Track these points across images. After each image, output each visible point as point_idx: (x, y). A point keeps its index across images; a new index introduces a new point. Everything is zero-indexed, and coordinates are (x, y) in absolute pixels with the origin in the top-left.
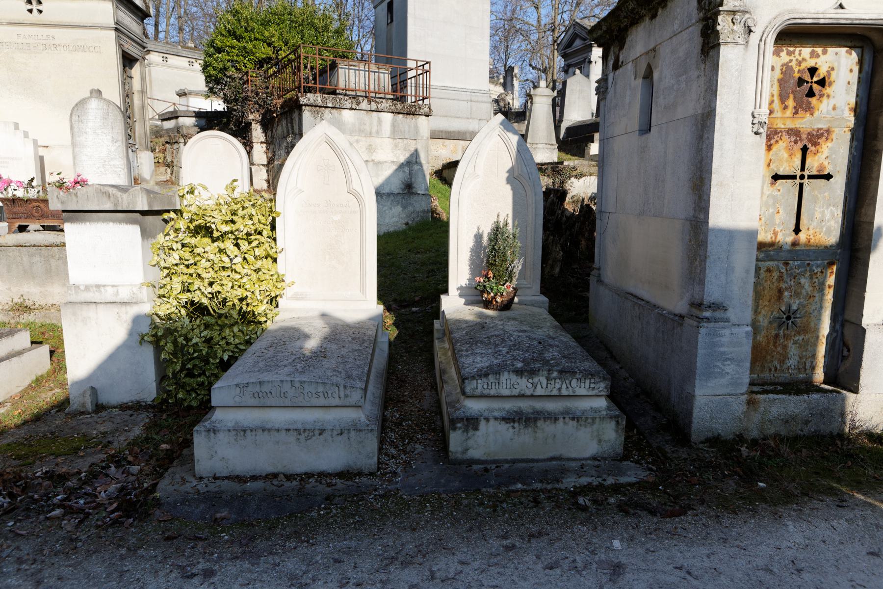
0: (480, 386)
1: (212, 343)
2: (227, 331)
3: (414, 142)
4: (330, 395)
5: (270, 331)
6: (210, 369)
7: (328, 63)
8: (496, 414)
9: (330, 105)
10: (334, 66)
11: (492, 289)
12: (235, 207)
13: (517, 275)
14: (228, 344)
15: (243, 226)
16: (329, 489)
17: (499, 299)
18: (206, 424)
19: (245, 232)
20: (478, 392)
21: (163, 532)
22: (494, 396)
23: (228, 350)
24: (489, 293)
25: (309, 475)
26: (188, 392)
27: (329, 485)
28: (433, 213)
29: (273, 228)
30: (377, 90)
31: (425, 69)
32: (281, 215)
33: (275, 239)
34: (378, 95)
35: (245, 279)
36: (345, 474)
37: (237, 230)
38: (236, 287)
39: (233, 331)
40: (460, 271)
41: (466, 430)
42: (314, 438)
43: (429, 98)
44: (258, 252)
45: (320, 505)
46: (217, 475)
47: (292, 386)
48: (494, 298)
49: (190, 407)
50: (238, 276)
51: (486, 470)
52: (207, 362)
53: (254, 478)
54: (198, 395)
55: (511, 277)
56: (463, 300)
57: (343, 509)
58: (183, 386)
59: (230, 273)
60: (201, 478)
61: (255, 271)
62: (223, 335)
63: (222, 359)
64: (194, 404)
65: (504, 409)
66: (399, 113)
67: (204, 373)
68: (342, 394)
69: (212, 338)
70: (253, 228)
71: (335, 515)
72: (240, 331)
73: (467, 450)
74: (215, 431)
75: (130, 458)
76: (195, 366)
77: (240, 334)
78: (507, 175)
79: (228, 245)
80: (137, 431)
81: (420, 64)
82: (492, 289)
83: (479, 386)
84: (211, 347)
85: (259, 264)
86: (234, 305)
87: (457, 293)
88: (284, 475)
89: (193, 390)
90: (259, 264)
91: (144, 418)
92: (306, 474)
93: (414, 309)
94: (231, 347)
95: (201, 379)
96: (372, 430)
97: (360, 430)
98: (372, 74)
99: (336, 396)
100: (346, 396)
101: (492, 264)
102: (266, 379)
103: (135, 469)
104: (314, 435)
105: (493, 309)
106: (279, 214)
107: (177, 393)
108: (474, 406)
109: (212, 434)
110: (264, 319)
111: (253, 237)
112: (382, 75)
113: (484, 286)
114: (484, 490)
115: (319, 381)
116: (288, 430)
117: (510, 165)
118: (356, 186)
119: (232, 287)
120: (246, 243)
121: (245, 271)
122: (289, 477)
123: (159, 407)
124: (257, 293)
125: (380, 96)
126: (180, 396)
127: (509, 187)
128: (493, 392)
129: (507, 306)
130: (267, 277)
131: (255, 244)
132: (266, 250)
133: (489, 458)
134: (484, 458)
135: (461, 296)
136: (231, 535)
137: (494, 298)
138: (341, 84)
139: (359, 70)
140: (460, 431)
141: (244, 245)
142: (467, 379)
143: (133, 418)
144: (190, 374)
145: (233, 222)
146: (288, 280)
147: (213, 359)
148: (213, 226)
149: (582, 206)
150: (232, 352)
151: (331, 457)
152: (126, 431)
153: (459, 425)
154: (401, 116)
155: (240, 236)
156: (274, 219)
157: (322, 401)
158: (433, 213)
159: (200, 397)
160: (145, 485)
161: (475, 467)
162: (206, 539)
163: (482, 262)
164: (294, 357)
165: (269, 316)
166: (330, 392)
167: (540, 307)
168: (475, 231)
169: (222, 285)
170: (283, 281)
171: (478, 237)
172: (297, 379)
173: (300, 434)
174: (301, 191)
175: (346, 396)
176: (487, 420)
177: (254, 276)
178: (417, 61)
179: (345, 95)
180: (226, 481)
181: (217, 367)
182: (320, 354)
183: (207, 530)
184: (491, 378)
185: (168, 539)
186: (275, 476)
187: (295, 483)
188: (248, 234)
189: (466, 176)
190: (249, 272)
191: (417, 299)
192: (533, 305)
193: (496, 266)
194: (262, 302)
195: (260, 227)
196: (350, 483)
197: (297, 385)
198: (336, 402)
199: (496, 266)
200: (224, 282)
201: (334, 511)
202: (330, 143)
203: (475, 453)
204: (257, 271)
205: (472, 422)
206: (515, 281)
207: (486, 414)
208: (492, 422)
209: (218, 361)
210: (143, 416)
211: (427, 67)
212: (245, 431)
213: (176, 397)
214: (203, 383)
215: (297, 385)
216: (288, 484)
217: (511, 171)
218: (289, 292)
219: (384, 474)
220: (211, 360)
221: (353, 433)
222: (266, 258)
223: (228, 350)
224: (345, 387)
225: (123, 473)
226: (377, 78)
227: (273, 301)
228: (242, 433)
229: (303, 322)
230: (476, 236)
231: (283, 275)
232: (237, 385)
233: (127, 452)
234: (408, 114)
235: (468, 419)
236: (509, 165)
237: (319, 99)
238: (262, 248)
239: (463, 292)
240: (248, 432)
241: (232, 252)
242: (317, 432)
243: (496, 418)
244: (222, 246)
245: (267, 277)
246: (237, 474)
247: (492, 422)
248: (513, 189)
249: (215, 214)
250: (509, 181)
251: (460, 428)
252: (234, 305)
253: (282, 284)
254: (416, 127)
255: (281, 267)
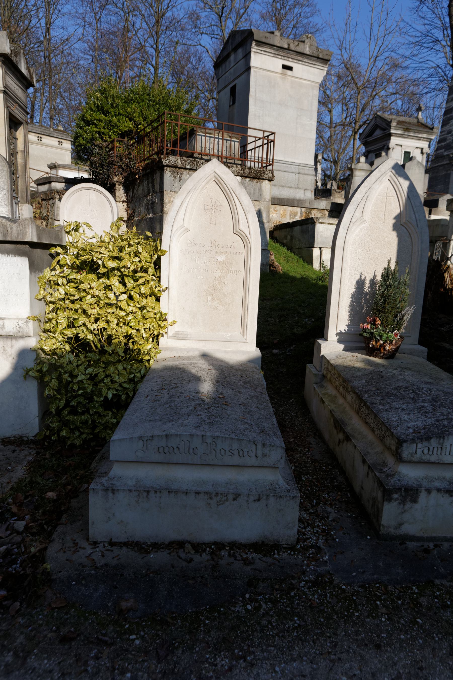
0: (419, 451)
1: (96, 380)
2: (112, 369)
3: (258, 203)
4: (245, 454)
5: (154, 370)
6: (94, 407)
7: (189, 130)
8: (437, 484)
9: (188, 167)
10: (192, 133)
11: (381, 337)
12: (122, 244)
13: (406, 323)
14: (112, 382)
15: (130, 264)
16: (248, 568)
17: (387, 347)
18: (104, 480)
19: (132, 269)
20: (416, 457)
21: (58, 628)
22: (434, 463)
23: (112, 389)
24: (377, 341)
25: (219, 546)
26: (72, 431)
27: (246, 562)
28: (270, 267)
29: (157, 264)
30: (228, 155)
31: (269, 140)
32: (167, 254)
33: (159, 277)
34: (228, 161)
35: (130, 317)
36: (262, 547)
37: (124, 267)
38: (121, 325)
39: (117, 369)
40: (339, 318)
41: (403, 503)
42: (227, 503)
43: (272, 165)
44: (143, 290)
45: (244, 597)
46: (114, 540)
47: (203, 441)
48: (382, 346)
49: (73, 446)
50: (123, 313)
51: (427, 551)
52: (91, 400)
53: (156, 546)
54: (82, 433)
55: (399, 325)
56: (342, 346)
57: (275, 602)
58: (66, 424)
59: (114, 310)
60: (95, 543)
61: (140, 308)
62: (108, 372)
63: (106, 398)
64: (78, 442)
65: (444, 478)
66: (246, 177)
67: (87, 411)
68: (259, 454)
69: (96, 375)
70: (140, 265)
71: (267, 613)
72: (125, 369)
73: (402, 524)
74: (113, 491)
75: (14, 509)
76: (79, 403)
77: (124, 372)
78: (393, 221)
79: (115, 281)
80: (20, 472)
81: (266, 134)
82: (381, 337)
83: (418, 450)
84: (95, 385)
85: (144, 302)
86: (120, 342)
87: (336, 338)
88: (193, 545)
89: (77, 428)
90: (144, 302)
91: (27, 455)
92: (215, 543)
93: (275, 351)
94: (116, 385)
95: (85, 417)
96: (294, 497)
97: (281, 497)
98: (225, 141)
99: (253, 455)
100: (264, 455)
101: (379, 311)
102: (173, 431)
103: (20, 525)
104: (227, 500)
105: (379, 357)
106: (164, 253)
107: (60, 430)
108: (410, 473)
109: (110, 494)
110: (147, 358)
111: (138, 275)
112: (233, 143)
113: (372, 333)
114: (437, 582)
115: (234, 436)
116: (197, 493)
117: (398, 211)
118: (243, 227)
119: (118, 324)
120: (132, 281)
121: (130, 309)
122: (198, 547)
123: (40, 443)
124: (142, 331)
125: (230, 161)
126: (64, 433)
127: (394, 234)
128: (433, 458)
129: (391, 356)
130: (152, 315)
131: (141, 281)
132: (151, 288)
133: (426, 535)
134: (419, 534)
135: (339, 341)
136: (142, 638)
137: (382, 346)
138: (198, 149)
139: (214, 138)
140: (396, 503)
141: (130, 283)
142: (405, 442)
143: (15, 454)
144: (74, 412)
145: (119, 259)
146: (170, 319)
147: (98, 397)
148: (100, 262)
149: (429, 262)
150: (117, 390)
151: (244, 525)
152: (8, 470)
153: (395, 496)
154: (248, 180)
155: (126, 273)
156: (159, 258)
157: (236, 460)
158: (270, 267)
159: (84, 436)
160: (33, 550)
161: (411, 545)
162: (112, 644)
163: (362, 308)
164: (193, 404)
165: (152, 354)
166: (246, 450)
167: (419, 356)
168: (357, 277)
169: (108, 322)
170: (166, 320)
171: (360, 283)
172: (209, 434)
173: (211, 498)
174: (188, 230)
175: (264, 455)
176: (429, 491)
177: (139, 315)
178: (264, 131)
179: (201, 159)
180: (125, 549)
181: (101, 406)
182: (218, 400)
183: (111, 628)
184: (434, 442)
185: (64, 640)
186: (180, 544)
187: (205, 557)
188: (135, 271)
189: (353, 220)
190: (135, 310)
191: (275, 341)
192: (411, 354)
193: (385, 313)
194: (147, 340)
195: (145, 265)
196: (269, 559)
197: (209, 440)
198: (252, 461)
199: (385, 313)
200: (109, 318)
201: (264, 606)
202: (219, 182)
203: (410, 529)
204: (142, 309)
205: (410, 493)
206: (402, 330)
207: (425, 484)
208: (434, 494)
209: (102, 399)
210: (26, 452)
211: (271, 137)
212: (148, 492)
213: (59, 435)
214: (87, 421)
215: (209, 440)
216: (197, 558)
217: (398, 218)
218: (171, 331)
219: (306, 549)
220: (95, 398)
221: (272, 500)
222: (150, 296)
223: (112, 389)
224: (264, 445)
225: (7, 529)
226: (228, 145)
227: (156, 338)
228: (145, 494)
229: (186, 362)
230: (358, 282)
231: (166, 314)
232: (140, 438)
233: (10, 500)
234: (254, 178)
235: (406, 490)
236: (397, 211)
237: (179, 161)
238: (148, 287)
239: (342, 338)
240: (152, 494)
241: (118, 289)
242: (231, 497)
243: (439, 490)
244: (108, 282)
245: (152, 315)
246: (136, 540)
247: (434, 494)
248: (398, 236)
249: (102, 250)
250: (395, 227)
251: (396, 499)
252: (120, 342)
253: (165, 323)
254: (260, 190)
255: (163, 306)
